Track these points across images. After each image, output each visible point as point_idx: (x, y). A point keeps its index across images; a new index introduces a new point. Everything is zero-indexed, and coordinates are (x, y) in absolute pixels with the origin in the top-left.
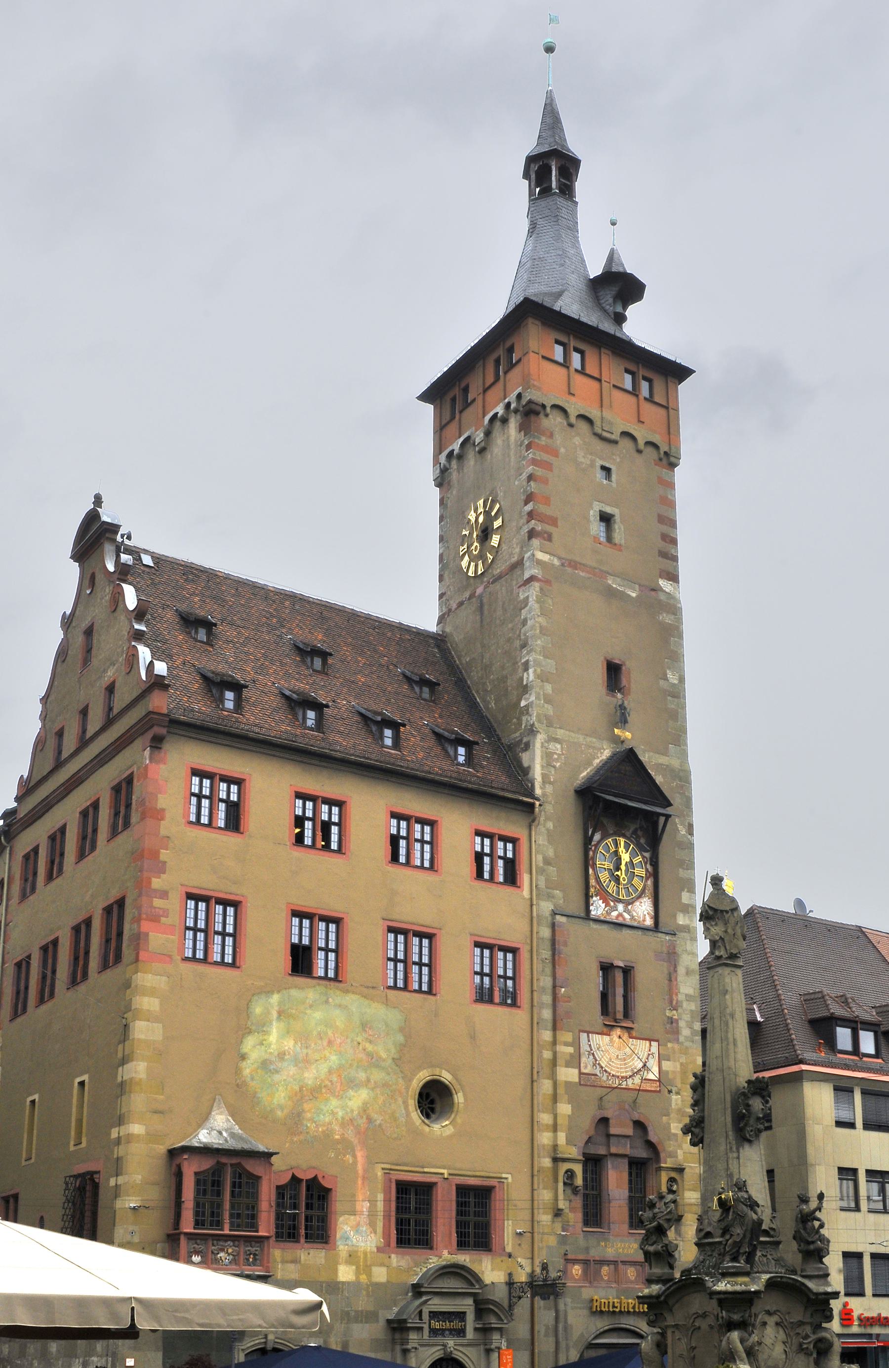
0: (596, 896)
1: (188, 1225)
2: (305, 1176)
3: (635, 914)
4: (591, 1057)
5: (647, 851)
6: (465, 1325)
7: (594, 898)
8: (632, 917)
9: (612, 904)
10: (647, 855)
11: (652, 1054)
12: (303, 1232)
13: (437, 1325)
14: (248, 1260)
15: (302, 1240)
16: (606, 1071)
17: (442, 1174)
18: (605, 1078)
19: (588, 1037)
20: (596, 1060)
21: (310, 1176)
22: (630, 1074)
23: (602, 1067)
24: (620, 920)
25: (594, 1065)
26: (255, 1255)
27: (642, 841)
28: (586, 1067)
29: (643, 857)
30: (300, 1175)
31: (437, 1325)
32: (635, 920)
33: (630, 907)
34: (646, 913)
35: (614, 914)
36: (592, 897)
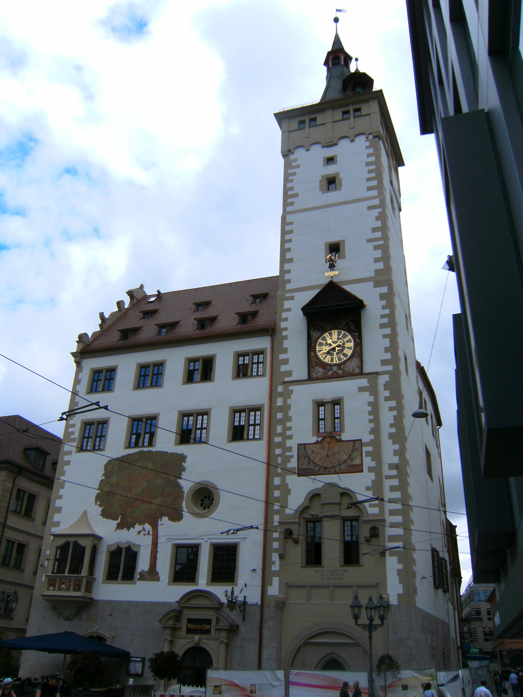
0: (316, 366)
1: (55, 571)
2: (123, 546)
3: (346, 369)
4: (307, 459)
5: (355, 332)
6: (210, 627)
7: (315, 368)
8: (344, 372)
9: (328, 368)
10: (356, 334)
11: (356, 449)
12: (120, 575)
13: (192, 626)
14: (75, 588)
15: (120, 578)
16: (318, 465)
17: (203, 539)
18: (317, 469)
19: (305, 447)
20: (310, 459)
21: (127, 545)
22: (338, 464)
23: (315, 463)
24: (335, 374)
25: (309, 463)
26: (79, 586)
27: (352, 327)
28: (303, 464)
29: (352, 336)
30: (121, 546)
31: (192, 626)
32: (346, 372)
33: (342, 366)
34: (355, 366)
35: (330, 373)
36: (314, 367)
